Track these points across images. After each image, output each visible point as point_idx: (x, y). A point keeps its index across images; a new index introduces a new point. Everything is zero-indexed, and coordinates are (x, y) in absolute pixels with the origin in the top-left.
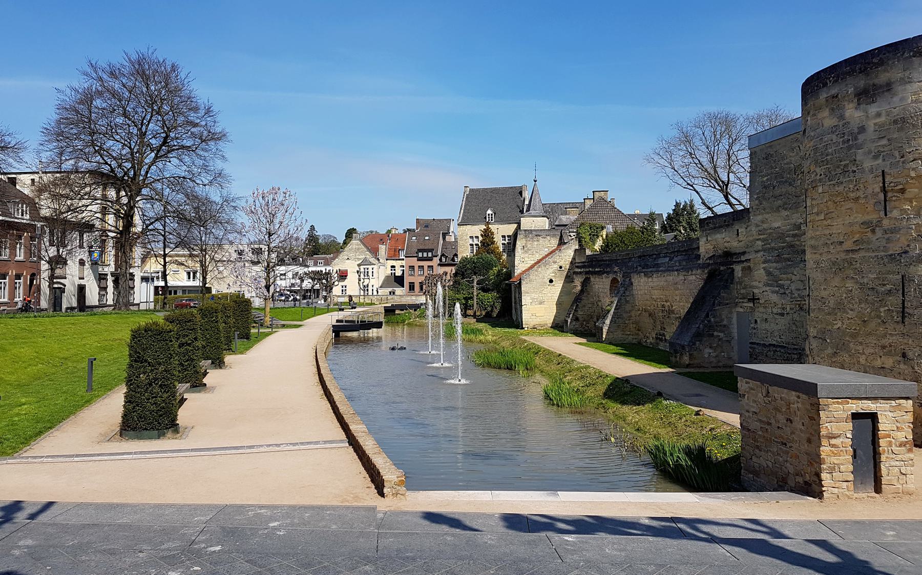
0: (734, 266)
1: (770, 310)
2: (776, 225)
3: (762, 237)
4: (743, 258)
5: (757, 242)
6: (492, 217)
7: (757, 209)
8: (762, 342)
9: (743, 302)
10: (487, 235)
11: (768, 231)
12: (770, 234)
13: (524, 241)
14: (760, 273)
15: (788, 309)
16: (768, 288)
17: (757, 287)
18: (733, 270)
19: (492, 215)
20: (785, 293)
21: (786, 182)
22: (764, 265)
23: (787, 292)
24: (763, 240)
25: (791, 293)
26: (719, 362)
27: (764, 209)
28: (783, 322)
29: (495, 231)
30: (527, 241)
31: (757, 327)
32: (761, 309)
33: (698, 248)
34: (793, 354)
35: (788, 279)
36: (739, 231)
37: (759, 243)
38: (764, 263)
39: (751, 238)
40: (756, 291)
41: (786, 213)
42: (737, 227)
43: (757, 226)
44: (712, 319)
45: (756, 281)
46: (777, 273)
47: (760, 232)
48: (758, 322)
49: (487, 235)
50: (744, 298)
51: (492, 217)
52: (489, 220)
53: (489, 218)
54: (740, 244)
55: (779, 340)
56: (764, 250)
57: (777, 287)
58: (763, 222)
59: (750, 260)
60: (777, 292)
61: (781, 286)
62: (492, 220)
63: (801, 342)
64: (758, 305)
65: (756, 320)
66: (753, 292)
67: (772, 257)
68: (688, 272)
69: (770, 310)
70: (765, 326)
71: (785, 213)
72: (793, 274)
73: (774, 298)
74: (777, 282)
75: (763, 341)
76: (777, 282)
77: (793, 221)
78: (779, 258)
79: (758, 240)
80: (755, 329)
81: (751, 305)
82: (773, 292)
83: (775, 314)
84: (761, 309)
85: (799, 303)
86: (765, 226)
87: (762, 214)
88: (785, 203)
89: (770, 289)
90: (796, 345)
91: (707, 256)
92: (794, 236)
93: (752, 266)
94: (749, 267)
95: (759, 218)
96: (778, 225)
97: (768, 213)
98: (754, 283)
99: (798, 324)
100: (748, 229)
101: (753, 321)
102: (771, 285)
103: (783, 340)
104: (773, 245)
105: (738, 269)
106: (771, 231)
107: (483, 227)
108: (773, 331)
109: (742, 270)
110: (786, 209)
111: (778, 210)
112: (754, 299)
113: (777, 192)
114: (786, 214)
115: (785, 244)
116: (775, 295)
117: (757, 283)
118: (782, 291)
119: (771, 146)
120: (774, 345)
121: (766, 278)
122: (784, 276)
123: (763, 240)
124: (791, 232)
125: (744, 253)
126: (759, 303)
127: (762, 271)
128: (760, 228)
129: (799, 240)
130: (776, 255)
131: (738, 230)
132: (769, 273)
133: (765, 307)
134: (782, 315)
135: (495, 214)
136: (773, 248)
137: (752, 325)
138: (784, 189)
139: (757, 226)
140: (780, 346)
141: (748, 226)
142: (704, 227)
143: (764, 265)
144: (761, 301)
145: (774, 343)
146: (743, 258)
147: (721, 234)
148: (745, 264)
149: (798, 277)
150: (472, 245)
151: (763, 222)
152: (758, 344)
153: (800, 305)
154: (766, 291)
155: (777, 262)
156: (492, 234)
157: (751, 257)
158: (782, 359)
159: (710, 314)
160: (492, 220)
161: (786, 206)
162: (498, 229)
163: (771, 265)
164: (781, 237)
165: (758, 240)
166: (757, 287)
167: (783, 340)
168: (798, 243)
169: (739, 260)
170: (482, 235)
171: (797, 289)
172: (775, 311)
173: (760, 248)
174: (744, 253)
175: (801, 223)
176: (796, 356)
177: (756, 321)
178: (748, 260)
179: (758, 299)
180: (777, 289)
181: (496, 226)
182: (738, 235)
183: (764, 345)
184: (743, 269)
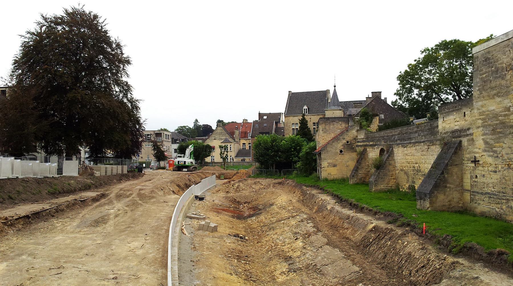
0: (462, 139)
1: (486, 169)
2: (492, 108)
3: (482, 117)
4: (468, 133)
6: (306, 111)
7: (479, 98)
8: (480, 191)
9: (467, 163)
10: (303, 123)
11: (486, 113)
12: (488, 115)
13: (324, 125)
14: (480, 143)
15: (500, 167)
17: (477, 153)
18: (461, 142)
19: (306, 109)
21: (500, 77)
22: (483, 137)
23: (499, 156)
24: (482, 119)
25: (502, 156)
26: (450, 205)
27: (484, 97)
28: (495, 177)
29: (309, 120)
30: (326, 125)
31: (477, 181)
32: (480, 168)
33: (437, 126)
34: (503, 199)
35: (500, 147)
36: (466, 114)
37: (480, 121)
38: (483, 135)
39: (474, 118)
40: (477, 155)
42: (464, 111)
43: (478, 109)
44: (446, 176)
45: (477, 148)
46: (492, 142)
47: (481, 114)
48: (478, 177)
49: (303, 123)
50: (469, 160)
51: (306, 111)
52: (305, 113)
53: (305, 111)
54: (466, 123)
55: (493, 190)
56: (483, 126)
57: (492, 152)
58: (482, 106)
60: (491, 156)
61: (495, 152)
62: (306, 113)
63: (509, 191)
65: (476, 175)
66: (475, 156)
67: (489, 131)
69: (486, 169)
71: (498, 99)
72: (504, 142)
73: (490, 160)
74: (492, 148)
75: (481, 190)
76: (492, 148)
77: (504, 105)
79: (478, 119)
80: (476, 182)
81: (473, 165)
82: (489, 156)
83: (491, 171)
84: (480, 168)
85: (508, 163)
86: (484, 109)
87: (482, 101)
88: (499, 92)
89: (487, 154)
90: (505, 193)
91: (444, 131)
92: (505, 115)
93: (474, 137)
94: (473, 140)
95: (480, 103)
96: (493, 109)
98: (476, 150)
99: (507, 178)
100: (472, 112)
101: (474, 177)
102: (488, 151)
103: (496, 190)
104: (489, 122)
105: (465, 141)
106: (488, 113)
107: (301, 118)
108: (489, 183)
109: (468, 141)
110: (499, 97)
112: (475, 161)
113: (493, 84)
114: (499, 100)
115: (498, 122)
116: (491, 158)
117: (478, 149)
118: (496, 155)
119: (489, 52)
120: (489, 193)
121: (484, 146)
122: (498, 145)
123: (482, 119)
124: (503, 113)
125: (469, 129)
126: (479, 164)
129: (508, 119)
130: (491, 129)
131: (465, 113)
132: (486, 143)
133: (483, 167)
134: (495, 172)
135: (308, 109)
136: (489, 125)
137: (474, 180)
138: (499, 82)
140: (493, 194)
141: (472, 110)
142: (442, 111)
143: (483, 137)
144: (480, 163)
145: (489, 191)
146: (468, 133)
147: (453, 116)
149: (507, 145)
150: (293, 129)
152: (477, 193)
154: (484, 155)
155: (492, 135)
156: (307, 122)
158: (495, 203)
159: (444, 172)
160: (306, 113)
161: (499, 94)
162: (310, 118)
164: (496, 116)
166: (477, 153)
167: (496, 190)
168: (507, 121)
170: (300, 123)
172: (490, 169)
173: (480, 125)
174: (469, 129)
175: (510, 106)
176: (504, 201)
177: (476, 177)
178: (471, 134)
179: (479, 161)
180: (492, 154)
181: (309, 117)
182: (465, 116)
183: (482, 193)
184: (468, 140)
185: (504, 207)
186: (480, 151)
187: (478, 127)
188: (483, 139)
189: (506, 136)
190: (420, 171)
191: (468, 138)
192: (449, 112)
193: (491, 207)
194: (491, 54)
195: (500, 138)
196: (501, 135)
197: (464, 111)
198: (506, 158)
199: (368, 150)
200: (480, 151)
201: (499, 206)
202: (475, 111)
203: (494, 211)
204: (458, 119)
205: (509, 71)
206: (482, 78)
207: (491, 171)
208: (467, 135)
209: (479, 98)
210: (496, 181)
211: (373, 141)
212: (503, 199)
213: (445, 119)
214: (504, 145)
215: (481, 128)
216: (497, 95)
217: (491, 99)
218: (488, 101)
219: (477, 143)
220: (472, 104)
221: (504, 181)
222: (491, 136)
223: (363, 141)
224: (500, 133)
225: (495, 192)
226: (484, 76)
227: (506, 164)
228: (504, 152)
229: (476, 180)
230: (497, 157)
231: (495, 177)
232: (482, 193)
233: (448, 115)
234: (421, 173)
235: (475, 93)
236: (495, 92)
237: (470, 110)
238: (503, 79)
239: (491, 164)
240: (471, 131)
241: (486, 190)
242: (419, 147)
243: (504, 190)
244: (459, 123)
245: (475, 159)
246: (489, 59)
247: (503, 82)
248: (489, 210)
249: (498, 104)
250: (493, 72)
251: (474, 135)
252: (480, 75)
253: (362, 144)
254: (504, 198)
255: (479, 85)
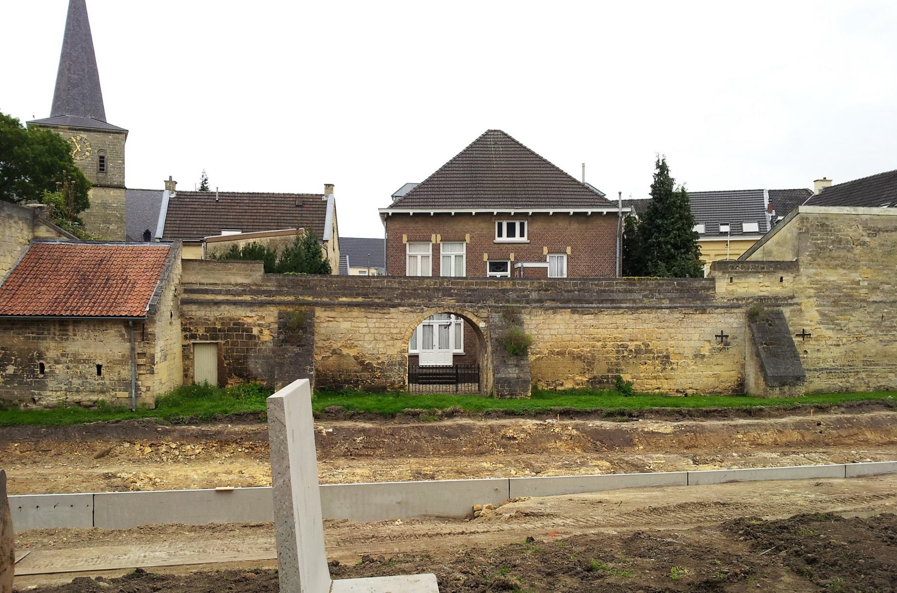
0: (781, 308)
2: (832, 279)
3: (815, 286)
4: (790, 301)
5: (809, 290)
11: (823, 283)
15: (844, 340)
16: (822, 326)
20: (842, 330)
21: (844, 248)
22: (818, 308)
23: (844, 329)
24: (816, 289)
35: (845, 320)
37: (812, 291)
38: (818, 306)
39: (801, 286)
40: (805, 328)
41: (844, 271)
42: (780, 275)
43: (809, 277)
45: (807, 320)
46: (834, 314)
47: (812, 283)
48: (809, 351)
54: (785, 289)
56: (818, 297)
57: (833, 325)
58: (816, 274)
59: (801, 303)
60: (833, 329)
61: (837, 324)
64: (810, 339)
68: (696, 310)
70: (816, 355)
72: (851, 315)
73: (830, 333)
77: (851, 278)
78: (836, 303)
79: (809, 288)
80: (804, 358)
81: (801, 339)
83: (832, 345)
92: (851, 288)
94: (801, 310)
95: (812, 271)
97: (823, 268)
100: (797, 278)
102: (827, 324)
104: (828, 293)
105: (787, 312)
106: (825, 283)
110: (844, 268)
111: (835, 267)
113: (835, 254)
118: (839, 328)
119: (827, 218)
122: (842, 317)
123: (816, 289)
125: (792, 298)
127: (816, 314)
128: (812, 279)
131: (782, 278)
132: (823, 314)
134: (838, 345)
139: (809, 277)
140: (835, 369)
143: (818, 308)
144: (812, 336)
146: (790, 301)
148: (795, 307)
149: (857, 318)
151: (816, 274)
153: (857, 338)
155: (833, 307)
157: (801, 301)
163: (827, 308)
164: (839, 288)
165: (809, 288)
168: (855, 294)
169: (786, 302)
171: (855, 327)
172: (829, 342)
173: (812, 294)
174: (792, 298)
175: (860, 281)
176: (853, 374)
179: (810, 334)
180: (833, 326)
183: (815, 370)
185: (851, 380)
186: (812, 323)
187: (810, 297)
188: (817, 311)
189: (855, 309)
190: (651, 351)
191: (792, 308)
192: (747, 272)
193: (830, 382)
194: (831, 222)
195: (845, 310)
196: (846, 308)
197: (780, 275)
198: (854, 331)
199: (317, 314)
200: (812, 323)
201: (844, 380)
202: (804, 279)
203: (837, 386)
204: (767, 284)
205: (857, 245)
206: (815, 244)
207: (832, 345)
208: (791, 305)
209: (810, 264)
210: (839, 354)
211: (365, 295)
212: (850, 372)
213: (734, 280)
214: (852, 318)
215: (815, 299)
216: (842, 266)
217: (831, 268)
218: (826, 270)
219: (807, 315)
220: (798, 270)
221: (851, 354)
222: (830, 308)
223: (252, 292)
224: (847, 305)
225: (836, 367)
226: (819, 242)
227: (853, 337)
228: (851, 325)
229: (805, 356)
230: (842, 330)
231: (836, 352)
232: (815, 370)
233: (746, 276)
234: (652, 355)
235: (805, 258)
236: (837, 262)
237: (794, 275)
238: (849, 251)
239: (830, 338)
240: (795, 300)
241: (822, 365)
242: (652, 316)
243: (850, 363)
244: (769, 289)
245: (803, 332)
246: (827, 226)
247: (849, 255)
248: (828, 386)
249: (842, 276)
250: (833, 242)
251: (803, 304)
252: (813, 239)
253: (220, 298)
254: (852, 371)
255: (811, 250)
